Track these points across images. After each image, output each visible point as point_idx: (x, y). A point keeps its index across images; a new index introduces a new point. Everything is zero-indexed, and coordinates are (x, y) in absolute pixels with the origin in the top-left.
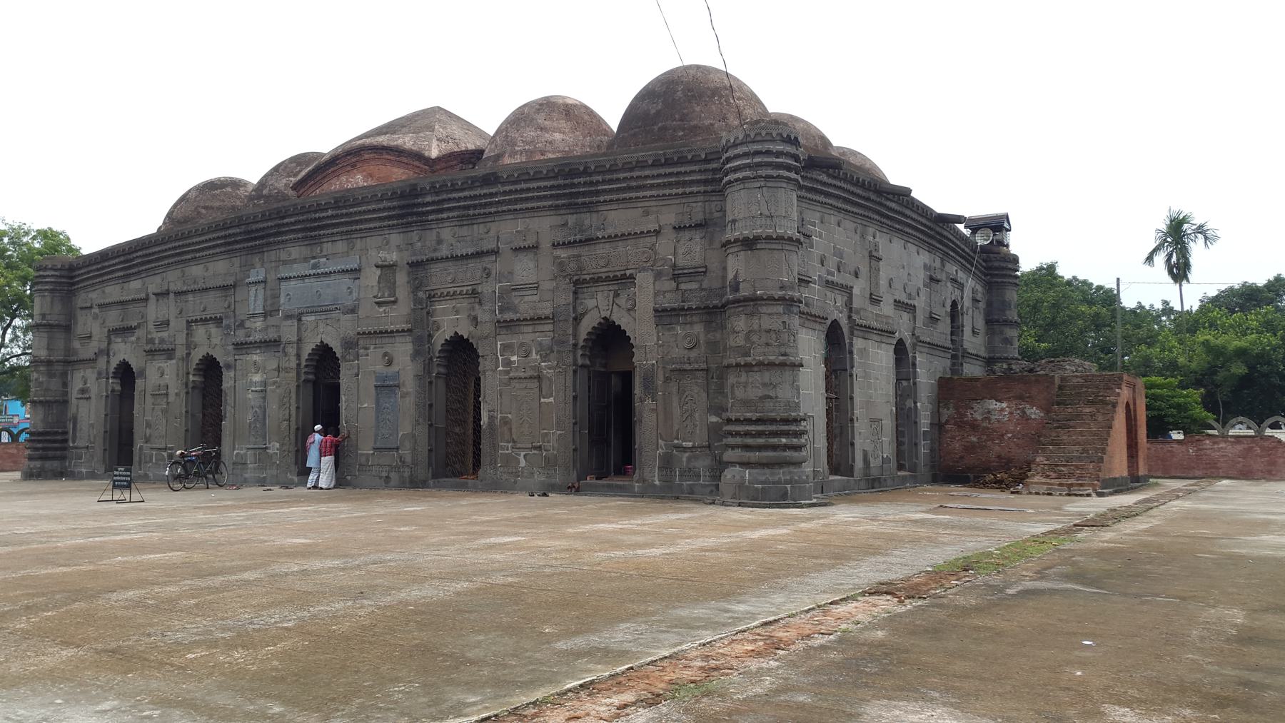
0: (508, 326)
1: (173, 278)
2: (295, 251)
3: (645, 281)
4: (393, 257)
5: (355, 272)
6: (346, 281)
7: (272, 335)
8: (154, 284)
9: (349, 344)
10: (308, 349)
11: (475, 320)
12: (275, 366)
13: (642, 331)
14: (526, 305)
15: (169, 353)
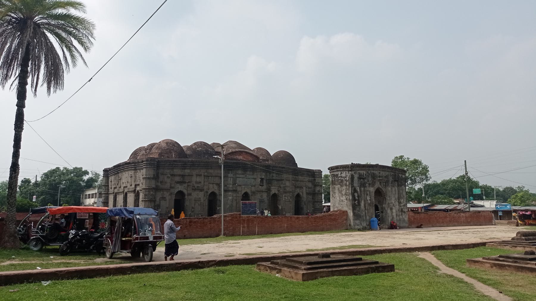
0: (285, 192)
1: (203, 172)
2: (240, 172)
3: (304, 188)
4: (263, 177)
5: (255, 179)
6: (253, 180)
7: (234, 188)
8: (194, 172)
9: (254, 193)
10: (243, 192)
11: (279, 191)
12: (235, 195)
13: (304, 196)
14: (288, 189)
15: (201, 190)
